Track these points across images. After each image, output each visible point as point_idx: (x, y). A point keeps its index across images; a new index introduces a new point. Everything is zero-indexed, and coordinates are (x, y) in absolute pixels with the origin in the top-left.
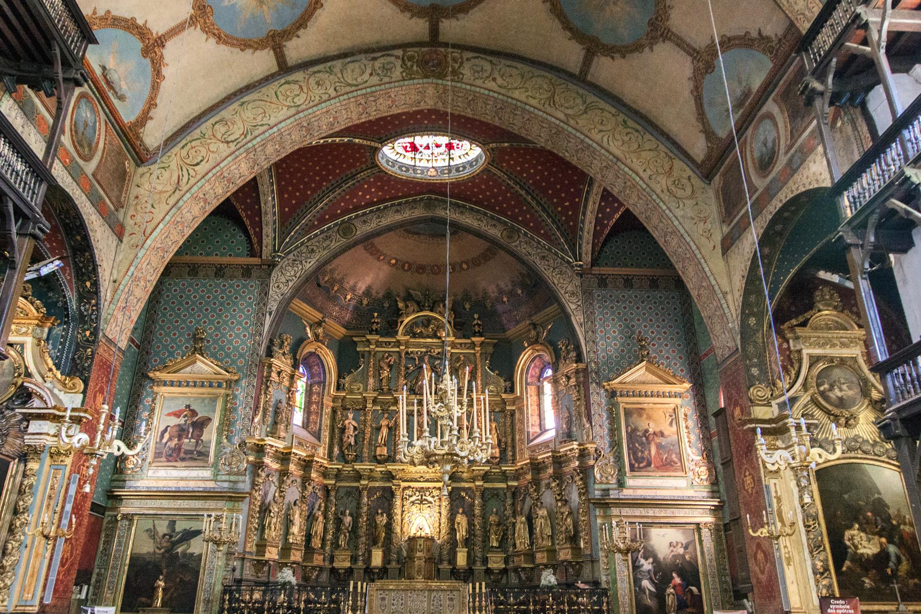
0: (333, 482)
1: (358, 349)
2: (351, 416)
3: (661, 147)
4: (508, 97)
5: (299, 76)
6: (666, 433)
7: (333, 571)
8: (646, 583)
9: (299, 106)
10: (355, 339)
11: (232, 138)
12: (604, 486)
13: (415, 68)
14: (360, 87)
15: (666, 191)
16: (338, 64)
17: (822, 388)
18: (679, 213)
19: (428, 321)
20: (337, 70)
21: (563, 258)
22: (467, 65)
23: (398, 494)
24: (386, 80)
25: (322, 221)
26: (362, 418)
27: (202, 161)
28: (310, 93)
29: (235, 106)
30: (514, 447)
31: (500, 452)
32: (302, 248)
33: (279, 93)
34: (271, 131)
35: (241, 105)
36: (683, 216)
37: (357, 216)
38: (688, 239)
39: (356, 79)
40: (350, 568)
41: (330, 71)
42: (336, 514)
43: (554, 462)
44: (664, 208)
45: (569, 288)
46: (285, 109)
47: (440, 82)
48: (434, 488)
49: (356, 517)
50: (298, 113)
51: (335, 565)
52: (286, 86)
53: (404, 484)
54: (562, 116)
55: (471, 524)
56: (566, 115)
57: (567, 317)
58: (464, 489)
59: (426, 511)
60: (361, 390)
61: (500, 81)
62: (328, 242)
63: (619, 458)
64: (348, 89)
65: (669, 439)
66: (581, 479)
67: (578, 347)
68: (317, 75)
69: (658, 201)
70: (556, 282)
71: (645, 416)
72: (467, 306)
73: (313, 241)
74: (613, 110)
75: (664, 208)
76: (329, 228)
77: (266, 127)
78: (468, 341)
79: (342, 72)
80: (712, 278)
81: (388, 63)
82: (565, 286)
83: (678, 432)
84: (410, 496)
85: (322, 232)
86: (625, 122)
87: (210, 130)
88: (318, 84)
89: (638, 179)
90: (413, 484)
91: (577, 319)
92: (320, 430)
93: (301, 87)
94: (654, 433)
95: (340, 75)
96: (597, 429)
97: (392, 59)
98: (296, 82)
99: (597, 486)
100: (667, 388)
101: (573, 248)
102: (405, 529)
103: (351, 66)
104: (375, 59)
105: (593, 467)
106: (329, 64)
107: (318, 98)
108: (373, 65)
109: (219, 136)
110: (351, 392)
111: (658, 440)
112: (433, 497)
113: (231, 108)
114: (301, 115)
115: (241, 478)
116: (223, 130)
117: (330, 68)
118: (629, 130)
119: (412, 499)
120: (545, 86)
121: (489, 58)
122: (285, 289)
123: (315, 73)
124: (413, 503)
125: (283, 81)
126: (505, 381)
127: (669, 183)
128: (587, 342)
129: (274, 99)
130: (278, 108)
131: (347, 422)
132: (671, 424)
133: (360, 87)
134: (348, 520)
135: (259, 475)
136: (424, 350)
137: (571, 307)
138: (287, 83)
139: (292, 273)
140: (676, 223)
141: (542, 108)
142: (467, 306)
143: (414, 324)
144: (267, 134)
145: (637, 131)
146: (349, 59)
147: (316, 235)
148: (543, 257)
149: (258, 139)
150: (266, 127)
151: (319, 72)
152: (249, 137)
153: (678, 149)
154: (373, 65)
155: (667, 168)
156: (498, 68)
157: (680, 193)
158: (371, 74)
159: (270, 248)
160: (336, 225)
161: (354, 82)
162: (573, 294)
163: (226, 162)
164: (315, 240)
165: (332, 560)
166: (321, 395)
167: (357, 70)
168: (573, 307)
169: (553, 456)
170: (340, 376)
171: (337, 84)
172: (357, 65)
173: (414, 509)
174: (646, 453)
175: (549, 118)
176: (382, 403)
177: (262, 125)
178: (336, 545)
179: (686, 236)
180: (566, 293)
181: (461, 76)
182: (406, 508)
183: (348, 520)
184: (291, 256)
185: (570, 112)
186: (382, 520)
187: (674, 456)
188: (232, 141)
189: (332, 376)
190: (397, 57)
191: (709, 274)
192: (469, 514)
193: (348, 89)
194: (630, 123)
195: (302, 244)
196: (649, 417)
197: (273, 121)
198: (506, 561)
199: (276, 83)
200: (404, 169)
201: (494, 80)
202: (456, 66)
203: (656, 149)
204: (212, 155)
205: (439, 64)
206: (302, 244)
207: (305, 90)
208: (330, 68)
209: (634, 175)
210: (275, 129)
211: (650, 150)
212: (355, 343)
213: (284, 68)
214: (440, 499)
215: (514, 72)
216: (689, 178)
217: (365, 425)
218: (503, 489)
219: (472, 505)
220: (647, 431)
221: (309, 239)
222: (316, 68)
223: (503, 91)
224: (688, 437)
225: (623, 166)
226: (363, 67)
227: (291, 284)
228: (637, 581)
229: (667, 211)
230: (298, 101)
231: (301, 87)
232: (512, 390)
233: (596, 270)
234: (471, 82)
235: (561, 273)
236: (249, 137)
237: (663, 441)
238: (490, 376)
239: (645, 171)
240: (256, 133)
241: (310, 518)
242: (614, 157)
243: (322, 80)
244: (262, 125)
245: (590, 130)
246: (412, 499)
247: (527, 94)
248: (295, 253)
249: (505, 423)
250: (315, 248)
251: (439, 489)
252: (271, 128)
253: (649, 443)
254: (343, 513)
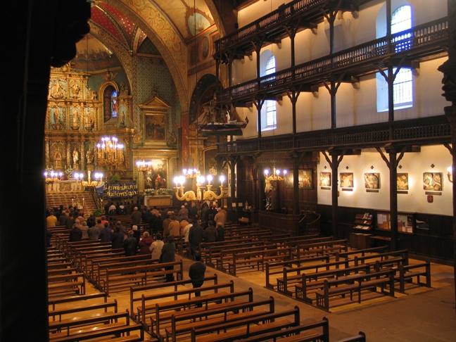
8: (149, 178)
57: (126, 75)
67: (129, 87)
74: (155, 9)
91: (129, 77)
94: (156, 126)
137: (127, 71)
148: (116, 47)
162: (128, 65)
185: (138, 8)
228: (145, 178)
233: (138, 54)
235: (124, 54)
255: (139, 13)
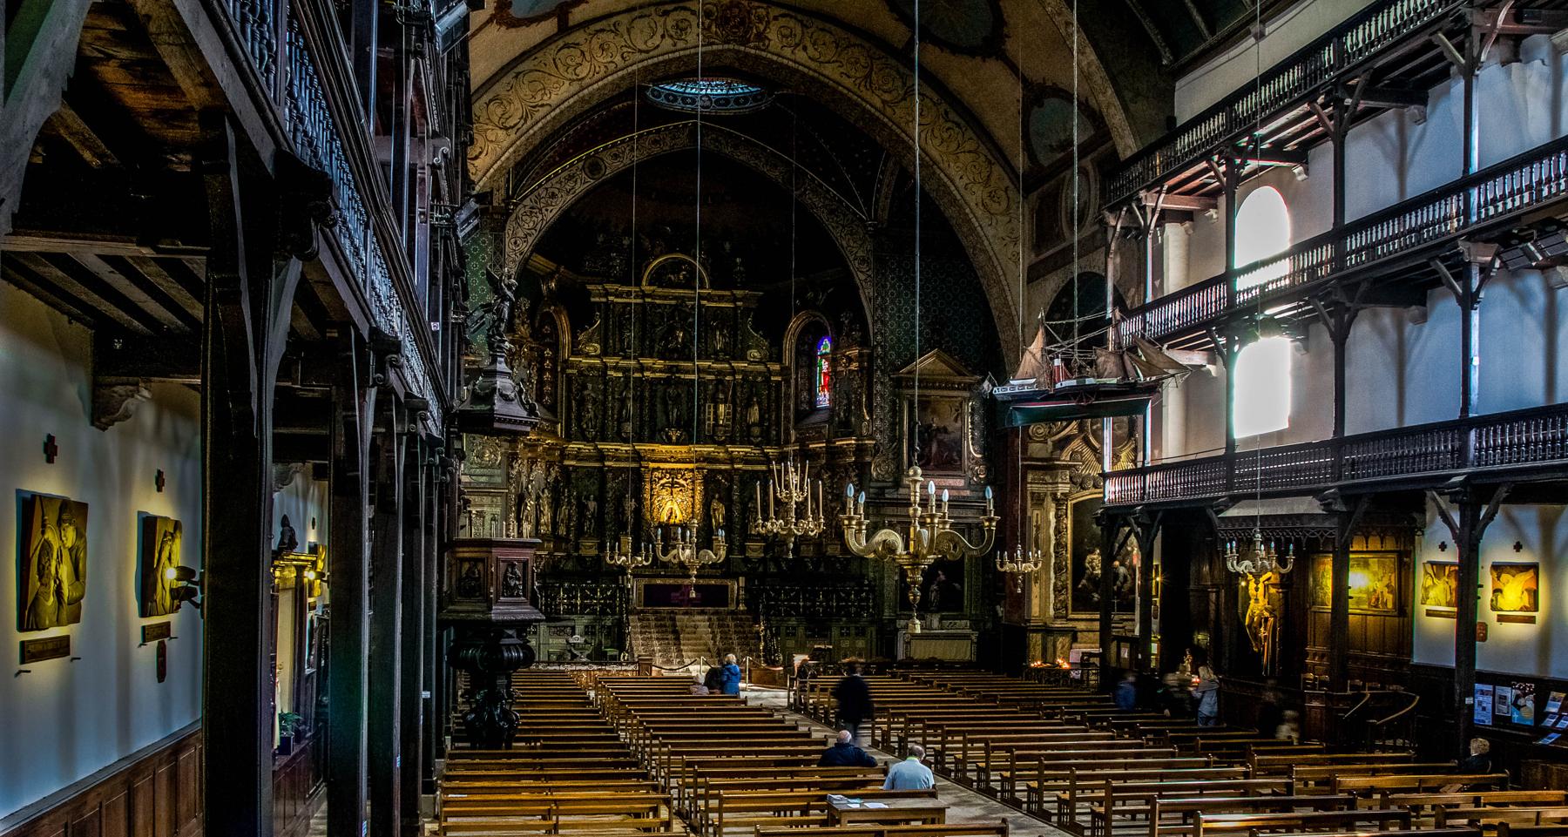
0: (573, 463)
1: (593, 300)
2: (590, 386)
3: (983, 149)
4: (819, 74)
5: (578, 36)
6: (950, 429)
7: (581, 559)
9: (583, 79)
10: (589, 287)
11: (511, 123)
12: (879, 485)
13: (714, 28)
14: (651, 54)
15: (980, 205)
16: (624, 19)
17: (1095, 427)
18: (990, 232)
19: (676, 266)
20: (622, 29)
21: (856, 214)
22: (774, 27)
23: (647, 476)
24: (681, 45)
25: (565, 156)
26: (602, 387)
27: (481, 153)
28: (594, 62)
29: (509, 78)
30: (778, 424)
31: (762, 432)
32: (540, 191)
33: (558, 62)
34: (553, 114)
35: (516, 77)
36: (994, 236)
37: (605, 148)
38: (996, 263)
39: (646, 43)
40: (597, 555)
41: (616, 32)
42: (578, 498)
43: (827, 452)
44: (977, 224)
45: (860, 254)
46: (567, 83)
47: (742, 48)
48: (686, 469)
49: (601, 500)
50: (582, 89)
51: (583, 552)
52: (566, 51)
53: (652, 465)
54: (879, 104)
55: (729, 510)
56: (884, 102)
58: (720, 472)
59: (679, 497)
60: (599, 352)
61: (811, 50)
62: (571, 184)
63: (898, 453)
64: (638, 56)
65: (952, 436)
66: (856, 476)
68: (601, 35)
69: (971, 216)
70: (845, 245)
71: (929, 410)
72: (727, 246)
73: (554, 181)
75: (977, 224)
76: (572, 165)
77: (547, 109)
78: (728, 293)
79: (628, 31)
80: (1013, 308)
81: (682, 21)
82: (855, 250)
83: (961, 429)
84: (660, 479)
85: (564, 170)
86: (946, 113)
87: (485, 112)
88: (601, 47)
89: (953, 188)
90: (662, 465)
91: (866, 292)
92: (555, 402)
93: (583, 53)
94: (938, 429)
95: (626, 37)
96: (878, 423)
97: (687, 15)
98: (577, 45)
99: (872, 484)
100: (958, 379)
101: (868, 203)
102: (654, 515)
103: (639, 24)
104: (666, 13)
105: (870, 464)
106: (614, 20)
107: (603, 69)
108: (665, 23)
109: (496, 119)
110: (588, 356)
111: (941, 437)
112: (686, 480)
113: (505, 80)
114: (586, 91)
115: (498, 472)
116: (499, 111)
117: (614, 25)
118: (949, 125)
119: (662, 482)
120: (862, 60)
121: (799, 17)
122: (525, 247)
123: (597, 32)
124: (663, 485)
125: (561, 43)
126: (771, 345)
127: (985, 195)
128: (875, 322)
129: (553, 71)
130: (557, 83)
131: (586, 392)
132: (956, 420)
133: (651, 54)
134: (592, 505)
135: (512, 468)
136: (673, 302)
137: (860, 277)
138: (567, 46)
139: (531, 224)
140: (986, 243)
141: (856, 90)
142: (727, 246)
143: (661, 269)
144: (548, 118)
145: (958, 125)
146: (636, 14)
147: (556, 174)
148: (832, 212)
149: (540, 125)
150: (547, 109)
151: (602, 31)
152: (529, 123)
153: (999, 155)
154: (665, 23)
155: (985, 174)
156: (810, 31)
157: (995, 207)
158: (663, 37)
159: (503, 191)
160: (579, 160)
161: (643, 47)
162: (863, 261)
163: (507, 155)
164: (557, 179)
165: (577, 548)
166: (554, 360)
167: (647, 31)
168: (862, 277)
169: (826, 447)
170: (574, 336)
171: (625, 49)
172: (646, 21)
173: (664, 492)
174: (927, 450)
175: (864, 104)
176: (626, 370)
177: (542, 106)
178: (580, 533)
179: (994, 259)
180: (854, 260)
181: (767, 42)
182: (655, 492)
183: (592, 505)
184: (527, 202)
185: (887, 97)
186: (630, 504)
187: (955, 454)
188: (512, 127)
189: (566, 339)
190: (693, 13)
191: (1011, 303)
192: (727, 501)
193: (638, 56)
194: (952, 116)
195: (540, 185)
196: (934, 412)
197: (554, 99)
198: (766, 550)
199: (553, 46)
200: (671, 98)
201: (805, 48)
202: (762, 27)
203: (975, 152)
204: (491, 146)
205: (742, 23)
206: (540, 185)
207: (588, 58)
208: (614, 25)
209: (949, 183)
210: (558, 111)
211: (970, 152)
212: (589, 294)
213: (564, 29)
214: (693, 482)
215: (828, 38)
216: (1007, 189)
217: (606, 397)
218: (762, 471)
219: (730, 489)
220: (931, 426)
221: (548, 180)
222: (598, 26)
223: (813, 65)
224: (972, 434)
225: (938, 171)
226: (653, 25)
227: (530, 239)
229: (979, 228)
230: (583, 71)
231: (583, 53)
232: (779, 360)
234: (779, 50)
236: (529, 123)
237: (945, 438)
238: (753, 337)
239: (961, 178)
240: (538, 115)
241: (555, 505)
242: (931, 159)
243: (606, 42)
244: (542, 106)
245: (908, 122)
246: (662, 482)
247: (842, 70)
248: (533, 197)
249: (769, 395)
250: (556, 191)
251: (692, 470)
252: (554, 110)
253: (931, 440)
254: (587, 498)
255: (889, 111)
